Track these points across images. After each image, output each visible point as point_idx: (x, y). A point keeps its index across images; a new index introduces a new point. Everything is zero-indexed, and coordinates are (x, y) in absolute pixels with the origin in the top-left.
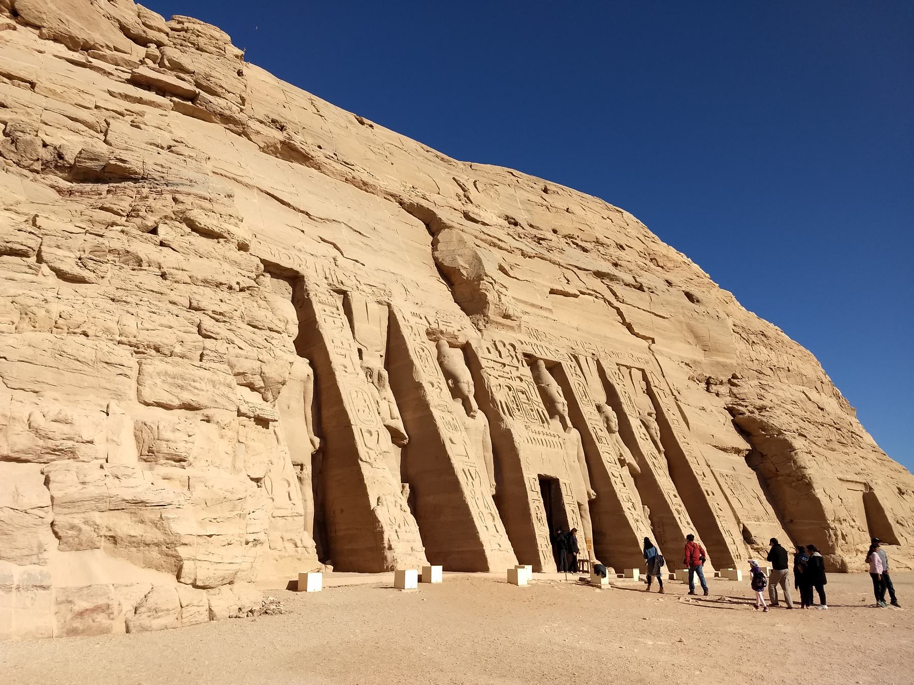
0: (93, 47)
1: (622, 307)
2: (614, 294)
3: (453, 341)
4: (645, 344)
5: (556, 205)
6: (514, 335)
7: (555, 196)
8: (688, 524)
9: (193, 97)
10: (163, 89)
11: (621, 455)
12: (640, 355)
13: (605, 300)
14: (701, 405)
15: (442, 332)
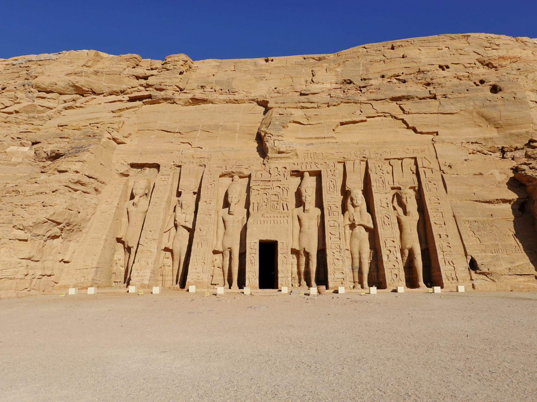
0: (124, 91)
1: (406, 117)
2: (403, 110)
3: (242, 175)
4: (431, 137)
5: (393, 56)
6: (291, 161)
7: (401, 48)
8: (397, 258)
9: (150, 97)
10: (140, 98)
11: (354, 220)
12: (416, 148)
13: (392, 116)
14: (477, 172)
15: (233, 172)
